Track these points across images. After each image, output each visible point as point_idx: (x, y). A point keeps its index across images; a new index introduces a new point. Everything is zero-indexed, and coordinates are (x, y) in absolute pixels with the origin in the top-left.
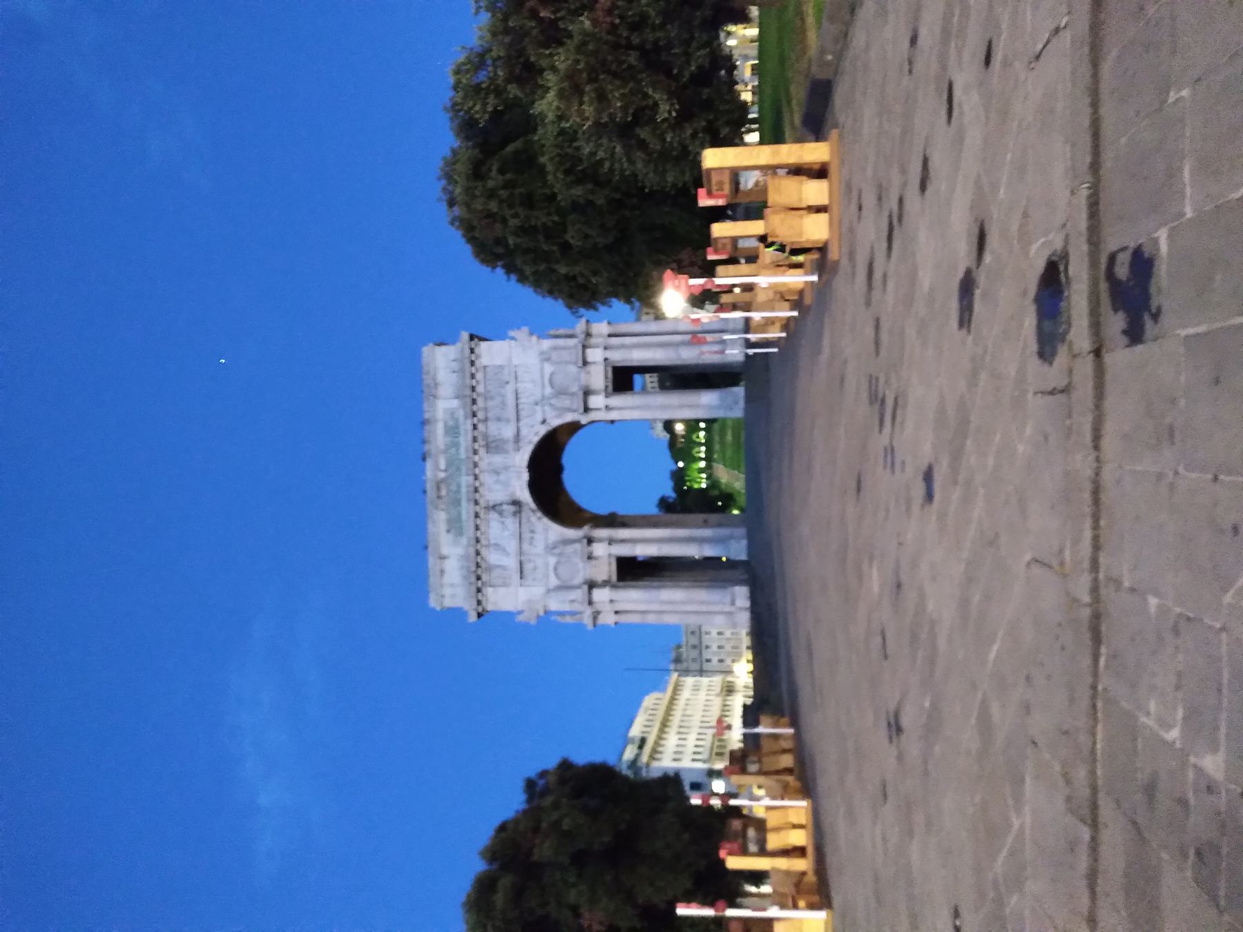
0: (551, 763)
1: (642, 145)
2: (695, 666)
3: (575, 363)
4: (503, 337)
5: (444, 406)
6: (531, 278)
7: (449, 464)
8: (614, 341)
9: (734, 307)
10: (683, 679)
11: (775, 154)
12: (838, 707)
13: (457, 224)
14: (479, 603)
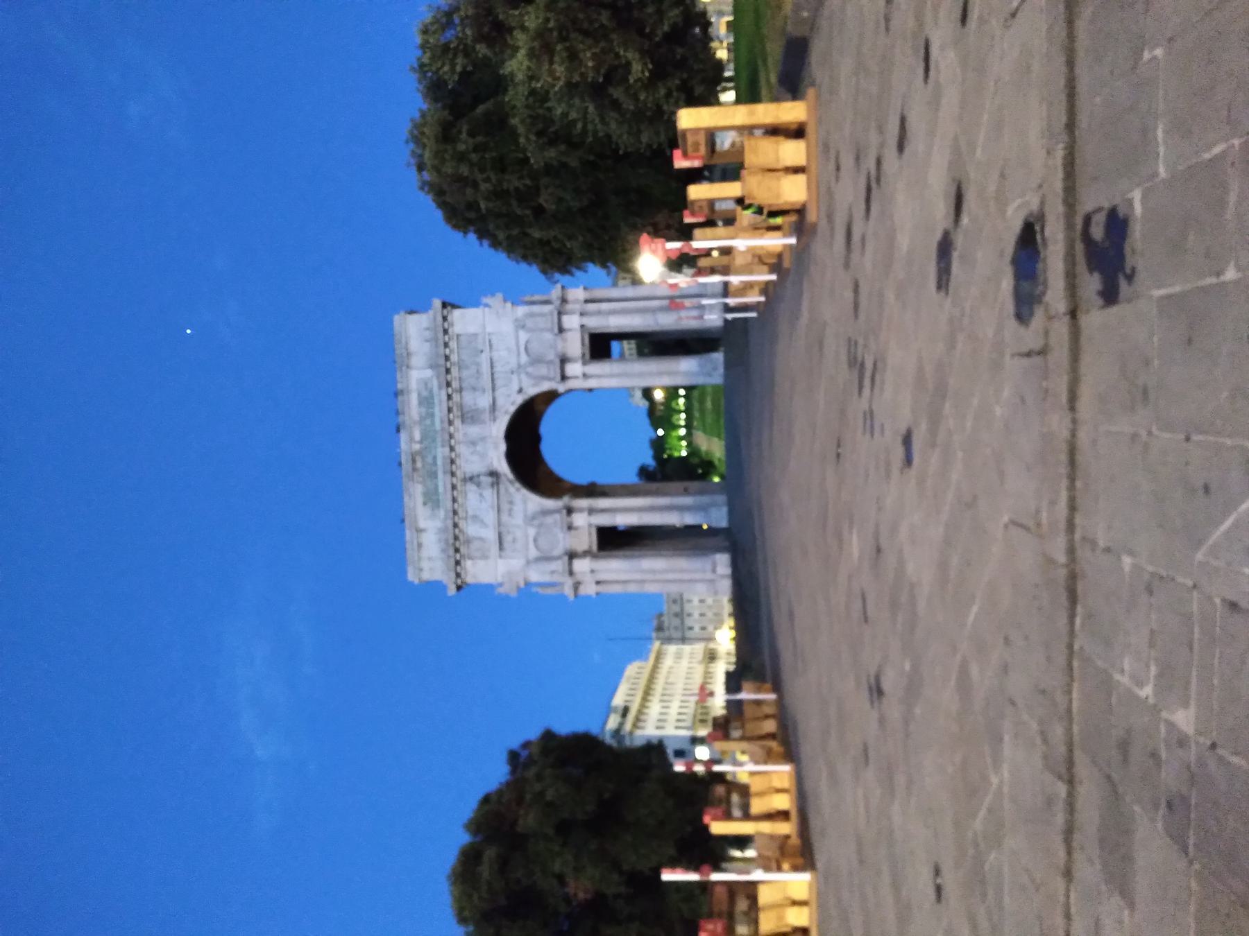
0: (534, 733)
1: (616, 105)
2: (678, 634)
3: (551, 330)
4: (476, 304)
5: (418, 375)
6: (504, 244)
8: (592, 307)
9: (712, 271)
10: (665, 647)
11: (752, 113)
12: (820, 672)
13: (426, 189)
14: (458, 575)
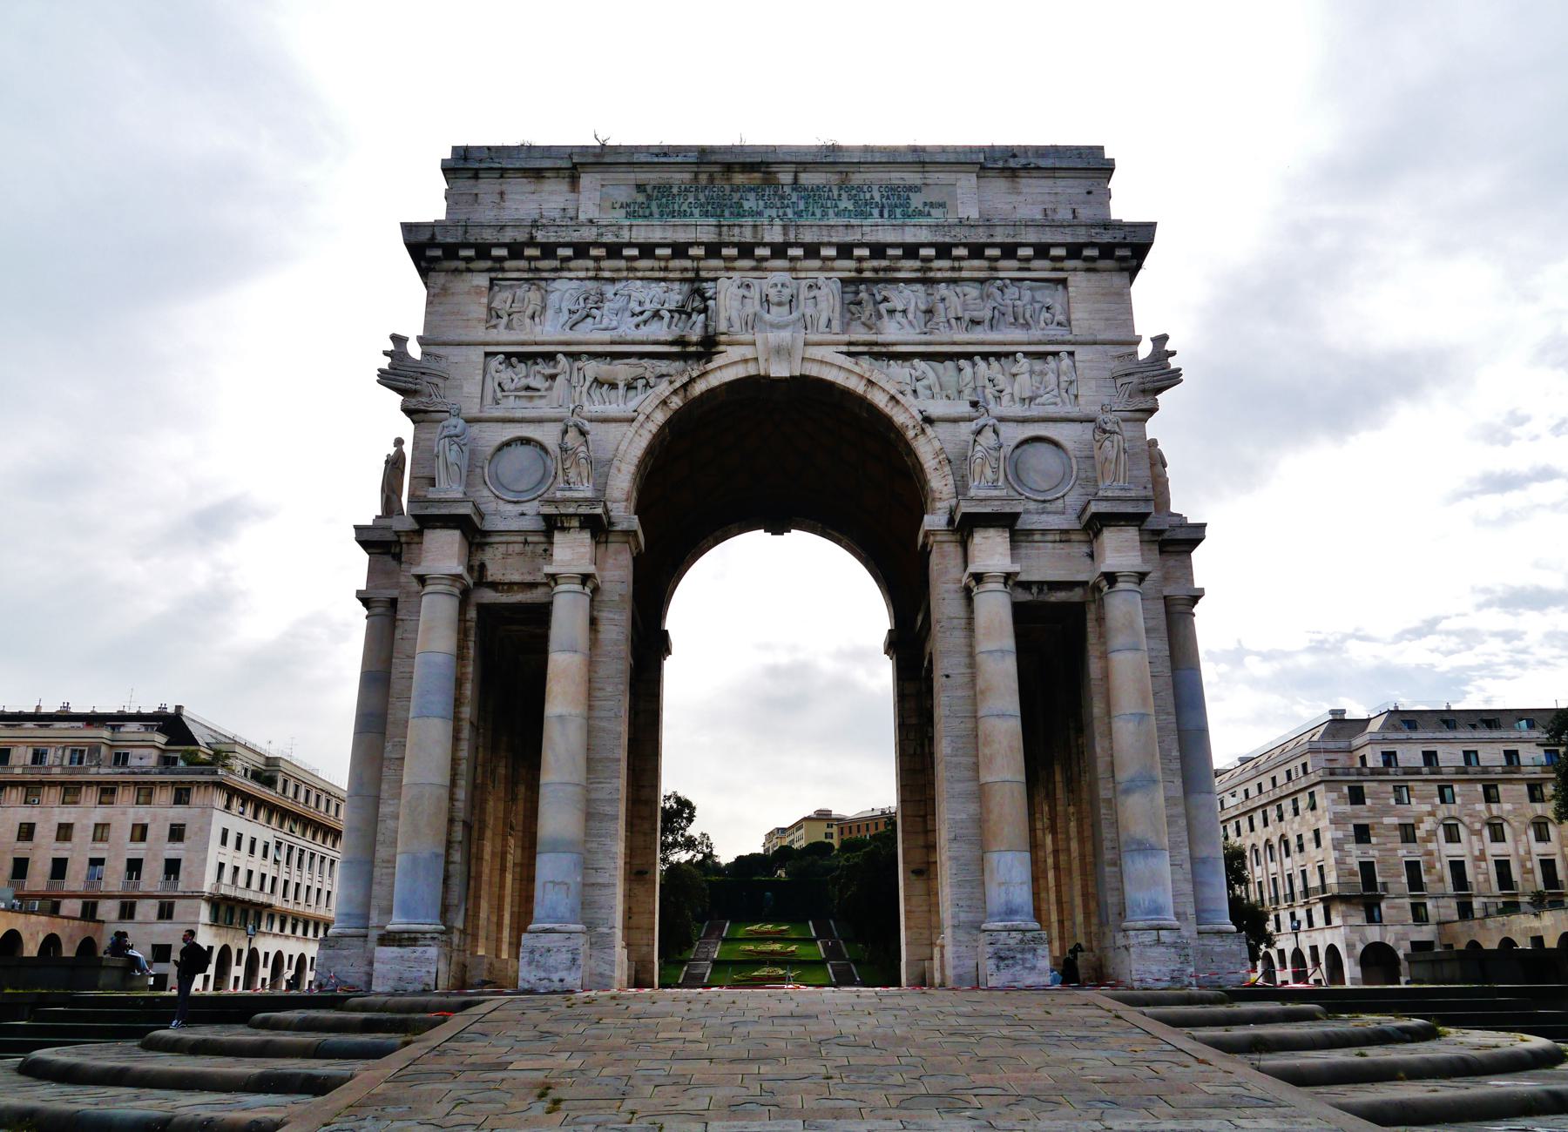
7: (813, 195)
14: (451, 251)
